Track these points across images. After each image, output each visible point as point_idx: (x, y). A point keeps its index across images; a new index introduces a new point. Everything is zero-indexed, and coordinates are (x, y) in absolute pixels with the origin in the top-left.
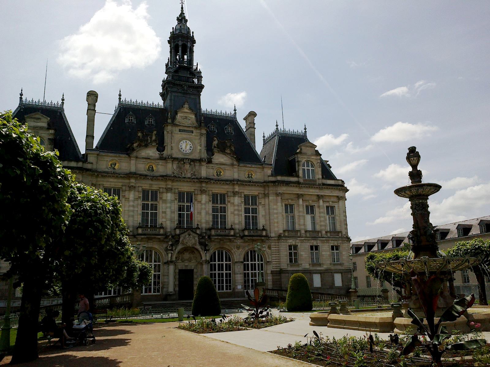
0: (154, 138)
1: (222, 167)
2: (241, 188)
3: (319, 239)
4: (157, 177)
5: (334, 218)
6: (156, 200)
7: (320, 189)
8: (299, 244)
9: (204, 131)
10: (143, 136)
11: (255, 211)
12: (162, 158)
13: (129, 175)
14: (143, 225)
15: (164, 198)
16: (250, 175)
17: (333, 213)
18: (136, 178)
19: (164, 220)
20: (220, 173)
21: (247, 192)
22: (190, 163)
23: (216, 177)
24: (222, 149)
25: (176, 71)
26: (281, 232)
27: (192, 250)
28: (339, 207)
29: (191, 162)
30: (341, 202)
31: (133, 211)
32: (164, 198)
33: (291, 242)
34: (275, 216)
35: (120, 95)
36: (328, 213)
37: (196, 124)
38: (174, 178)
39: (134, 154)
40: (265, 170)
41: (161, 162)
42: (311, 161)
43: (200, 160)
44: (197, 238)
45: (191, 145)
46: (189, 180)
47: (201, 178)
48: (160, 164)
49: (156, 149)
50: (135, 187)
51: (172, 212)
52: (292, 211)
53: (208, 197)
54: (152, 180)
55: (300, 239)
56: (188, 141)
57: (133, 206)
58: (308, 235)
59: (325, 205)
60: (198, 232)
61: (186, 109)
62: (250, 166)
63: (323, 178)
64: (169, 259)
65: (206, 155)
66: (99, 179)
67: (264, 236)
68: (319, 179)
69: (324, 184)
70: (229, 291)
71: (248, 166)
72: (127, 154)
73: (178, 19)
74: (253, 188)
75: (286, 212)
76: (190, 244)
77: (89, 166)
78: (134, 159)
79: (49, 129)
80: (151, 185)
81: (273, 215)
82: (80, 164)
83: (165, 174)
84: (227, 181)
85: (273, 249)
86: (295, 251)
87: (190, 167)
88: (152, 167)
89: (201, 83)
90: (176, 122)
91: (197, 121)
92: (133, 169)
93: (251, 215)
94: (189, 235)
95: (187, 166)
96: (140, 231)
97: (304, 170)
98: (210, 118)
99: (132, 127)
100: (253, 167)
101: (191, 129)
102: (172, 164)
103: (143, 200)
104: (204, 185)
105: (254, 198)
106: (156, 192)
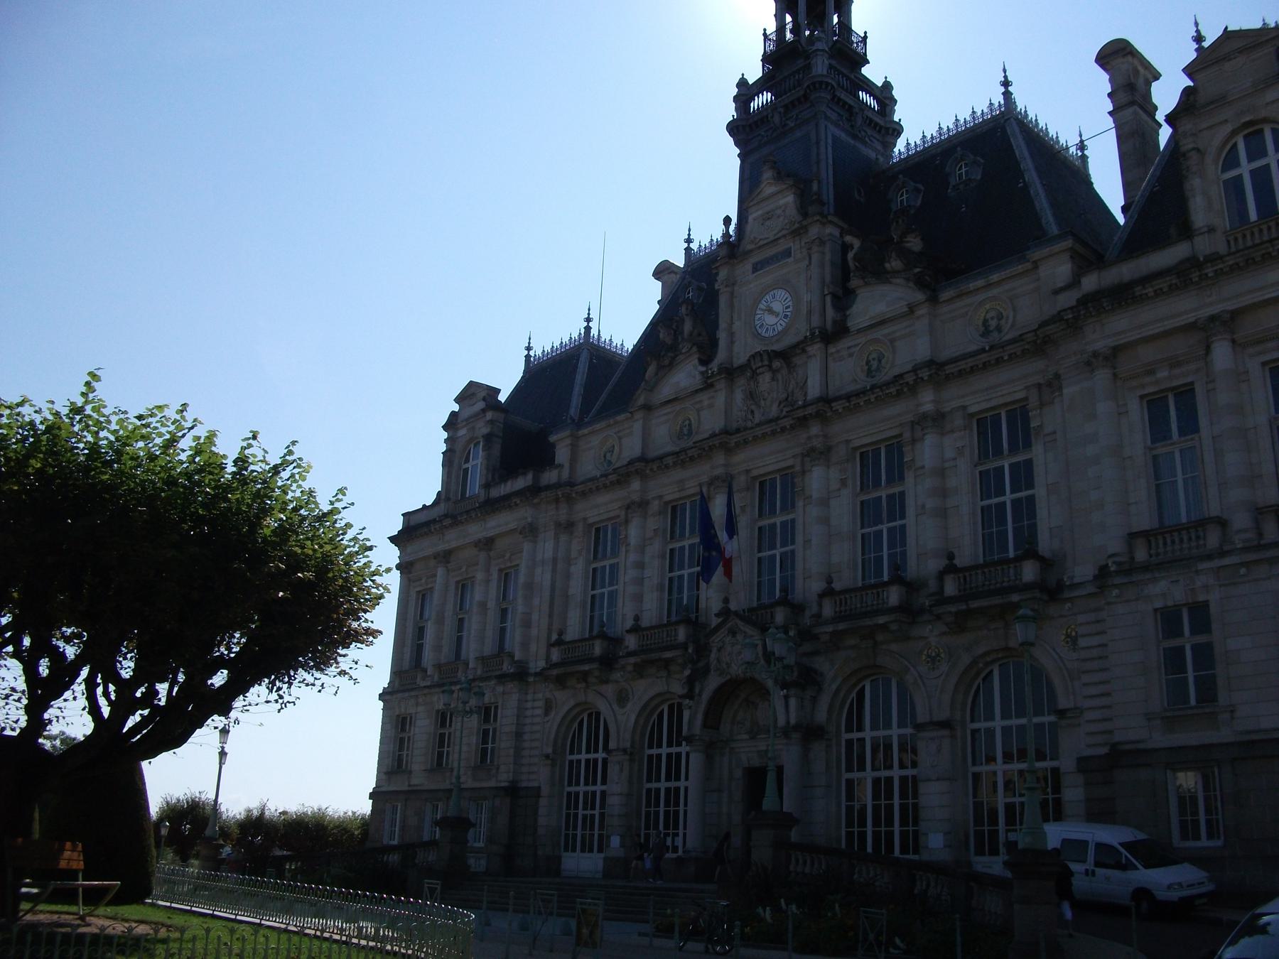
11: (1024, 475)
16: (993, 323)
20: (880, 361)
22: (770, 366)
26: (1116, 545)
29: (770, 361)
40: (1044, 271)
42: (1265, 120)
48: (706, 403)
52: (1190, 424)
62: (980, 283)
67: (1028, 587)
70: (911, 857)
71: (972, 286)
76: (736, 670)
78: (639, 415)
85: (1082, 642)
87: (773, 379)
88: (690, 425)
94: (733, 633)
95: (765, 380)
100: (999, 283)
104: (815, 429)
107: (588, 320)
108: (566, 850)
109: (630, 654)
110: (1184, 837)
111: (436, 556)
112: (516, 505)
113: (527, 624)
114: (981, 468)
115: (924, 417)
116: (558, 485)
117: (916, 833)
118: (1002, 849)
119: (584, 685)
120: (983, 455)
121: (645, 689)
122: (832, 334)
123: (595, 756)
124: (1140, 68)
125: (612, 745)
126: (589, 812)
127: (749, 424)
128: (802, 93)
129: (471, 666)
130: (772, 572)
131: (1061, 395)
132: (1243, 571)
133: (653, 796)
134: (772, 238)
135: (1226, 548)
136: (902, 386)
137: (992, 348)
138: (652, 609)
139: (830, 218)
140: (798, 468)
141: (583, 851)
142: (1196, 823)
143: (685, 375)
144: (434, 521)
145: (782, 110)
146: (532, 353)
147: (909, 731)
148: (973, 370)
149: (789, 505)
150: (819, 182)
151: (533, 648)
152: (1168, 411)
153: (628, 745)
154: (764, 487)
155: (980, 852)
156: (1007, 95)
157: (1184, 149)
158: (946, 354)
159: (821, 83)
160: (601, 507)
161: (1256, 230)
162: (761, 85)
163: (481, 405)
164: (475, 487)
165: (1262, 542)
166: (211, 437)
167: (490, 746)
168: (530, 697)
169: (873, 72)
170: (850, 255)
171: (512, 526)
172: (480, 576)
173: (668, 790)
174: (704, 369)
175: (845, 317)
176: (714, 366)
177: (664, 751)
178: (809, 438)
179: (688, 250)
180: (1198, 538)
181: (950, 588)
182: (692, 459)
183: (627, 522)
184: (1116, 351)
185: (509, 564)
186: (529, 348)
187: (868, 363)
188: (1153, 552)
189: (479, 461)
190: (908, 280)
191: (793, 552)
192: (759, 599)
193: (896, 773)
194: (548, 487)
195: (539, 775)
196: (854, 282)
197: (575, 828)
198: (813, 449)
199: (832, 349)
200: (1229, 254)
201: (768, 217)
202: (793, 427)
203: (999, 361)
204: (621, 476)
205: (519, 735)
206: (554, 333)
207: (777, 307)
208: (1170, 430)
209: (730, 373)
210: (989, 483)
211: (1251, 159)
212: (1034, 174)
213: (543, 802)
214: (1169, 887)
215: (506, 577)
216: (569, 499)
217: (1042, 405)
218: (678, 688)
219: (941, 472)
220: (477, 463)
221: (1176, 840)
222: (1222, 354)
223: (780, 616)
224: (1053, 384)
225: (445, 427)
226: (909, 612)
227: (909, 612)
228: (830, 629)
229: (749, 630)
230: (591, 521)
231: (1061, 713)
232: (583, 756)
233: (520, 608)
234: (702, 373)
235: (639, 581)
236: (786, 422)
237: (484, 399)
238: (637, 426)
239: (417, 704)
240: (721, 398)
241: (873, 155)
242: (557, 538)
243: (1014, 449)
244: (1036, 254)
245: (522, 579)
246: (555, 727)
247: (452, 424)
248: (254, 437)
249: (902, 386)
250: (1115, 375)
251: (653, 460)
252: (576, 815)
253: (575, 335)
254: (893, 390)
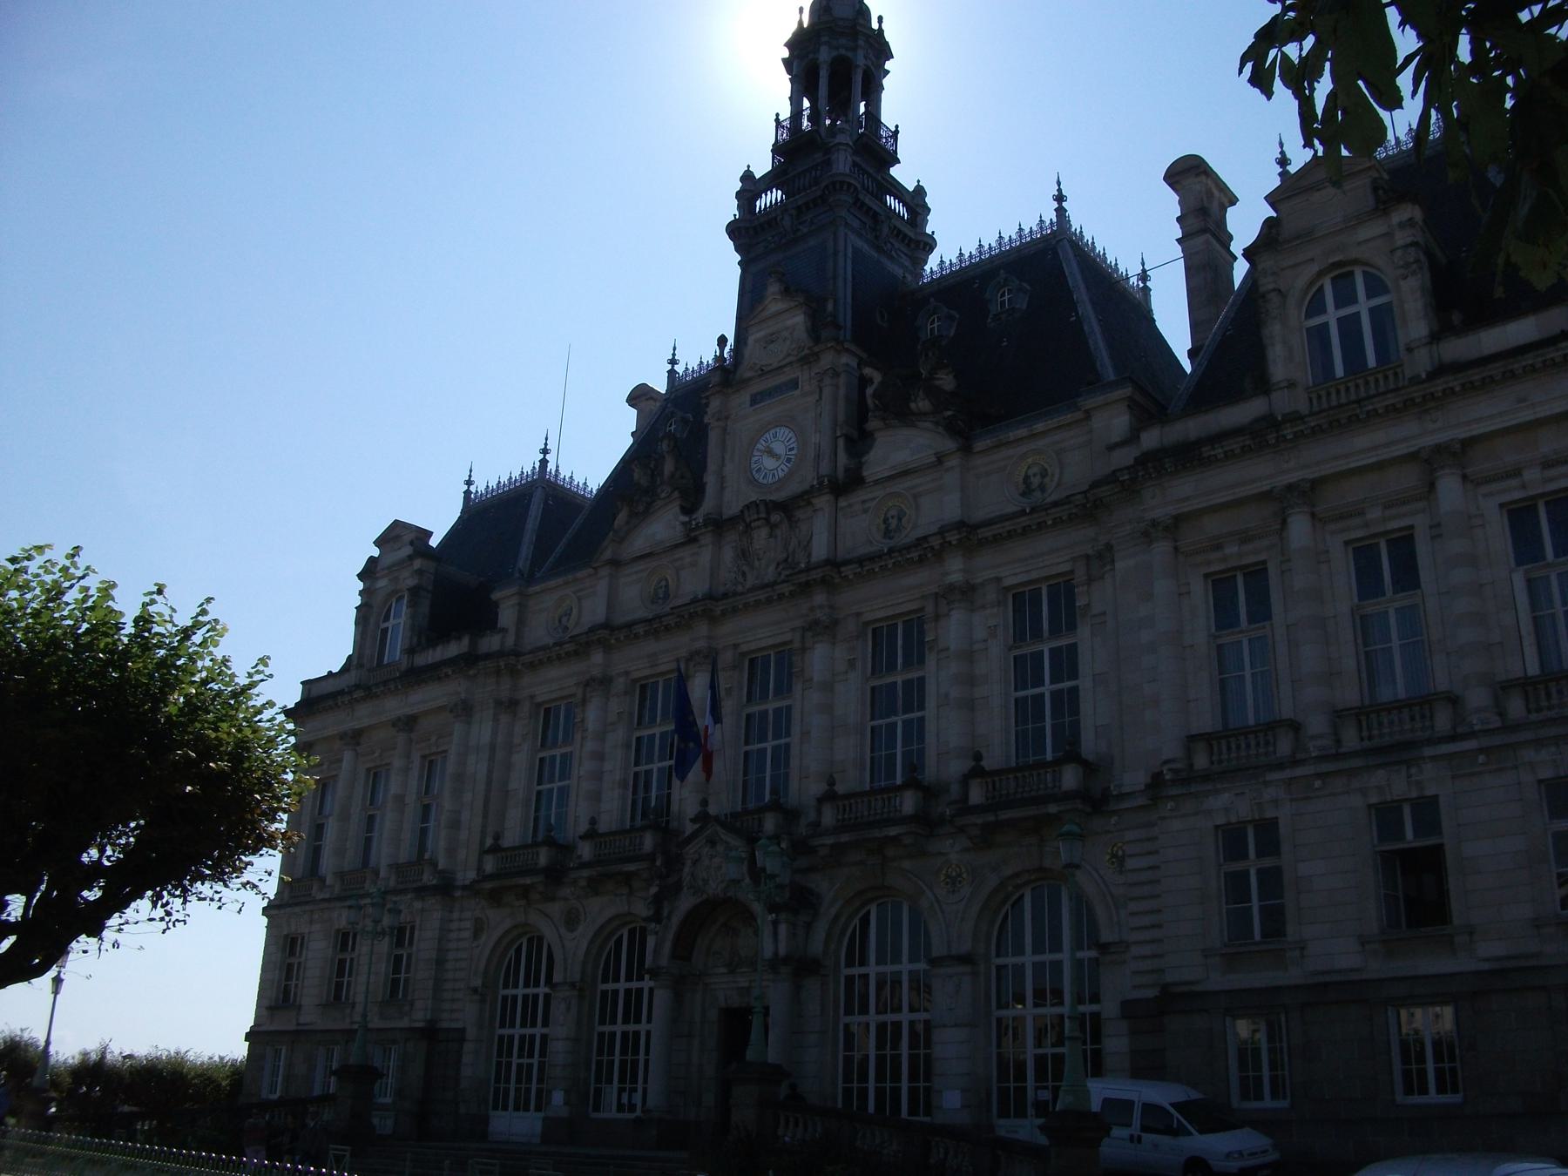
3: (1428, 751)
11: (1066, 663)
20: (900, 519)
22: (767, 520)
29: (768, 513)
42: (1356, 262)
46: (762, 596)
49: (677, 509)
52: (1261, 610)
55: (1288, 773)
62: (1022, 432)
67: (1068, 796)
70: (922, 1118)
71: (1012, 435)
78: (605, 572)
85: (1131, 863)
86: (1268, 862)
87: (771, 536)
88: (667, 586)
94: (712, 842)
95: (761, 536)
100: (1044, 433)
104: (820, 598)
107: (545, 451)
108: (495, 1108)
109: (584, 866)
110: (1245, 1096)
111: (342, 736)
112: (447, 676)
113: (455, 824)
114: (1017, 652)
115: (951, 588)
116: (500, 654)
117: (928, 1090)
118: (1030, 1111)
119: (523, 902)
120: (1019, 637)
121: (600, 909)
122: (846, 484)
123: (535, 990)
124: (1216, 192)
125: (557, 978)
126: (525, 1061)
127: (740, 589)
128: (819, 193)
129: (382, 874)
130: (761, 769)
131: (1113, 569)
132: (1318, 784)
133: (606, 1041)
134: (775, 365)
135: (1299, 756)
136: (926, 551)
137: (1033, 510)
138: (612, 810)
139: (846, 345)
140: (797, 645)
141: (517, 1109)
142: (1259, 1080)
143: (664, 525)
144: (341, 693)
145: (794, 212)
146: (473, 489)
147: (922, 966)
148: (1010, 535)
149: (783, 689)
150: (836, 302)
152: (1236, 593)
153: (577, 977)
154: (755, 664)
155: (1004, 1113)
156: (1061, 211)
157: (1262, 289)
158: (979, 515)
159: (842, 183)
160: (551, 683)
161: (1342, 388)
162: (770, 181)
163: (408, 550)
164: (395, 651)
165: (1342, 750)
166: (107, 589)
167: (403, 976)
168: (456, 915)
169: (903, 174)
170: (869, 391)
172: (397, 763)
173: (625, 1035)
174: (686, 519)
175: (860, 466)
176: (699, 516)
177: (622, 986)
178: (812, 609)
179: (672, 373)
180: (1267, 743)
181: (976, 795)
182: (667, 628)
183: (584, 702)
184: (1178, 519)
185: (434, 749)
186: (469, 483)
187: (886, 521)
188: (1215, 758)
189: (402, 621)
190: (937, 423)
191: (787, 746)
192: (744, 802)
193: (905, 1017)
194: (488, 656)
195: (464, 1014)
196: (873, 424)
197: (508, 1081)
198: (816, 622)
199: (843, 503)
200: (1312, 414)
201: (770, 340)
202: (792, 594)
203: (1041, 526)
204: (582, 645)
205: (440, 963)
206: (502, 466)
207: (779, 448)
208: (1237, 615)
209: (719, 525)
210: (1026, 671)
211: (1338, 305)
212: (1089, 308)
213: (468, 1047)
214: (1228, 1155)
215: (430, 765)
217: (1090, 581)
218: (641, 909)
219: (969, 656)
220: (400, 622)
221: (1236, 1102)
222: (1299, 528)
223: (770, 823)
224: (1104, 557)
225: (361, 576)
226: (926, 822)
227: (926, 822)
228: (829, 841)
230: (539, 700)
231: (1104, 948)
232: (521, 991)
234: (684, 523)
235: (598, 776)
236: (786, 589)
237: (412, 543)
238: (602, 586)
239: (311, 922)
240: (706, 557)
241: (899, 272)
242: (496, 720)
243: (1055, 632)
244: (1088, 403)
246: (487, 952)
247: (369, 572)
248: (160, 592)
249: (926, 551)
250: (1176, 549)
251: (620, 628)
252: (509, 1064)
253: (528, 469)
254: (915, 555)
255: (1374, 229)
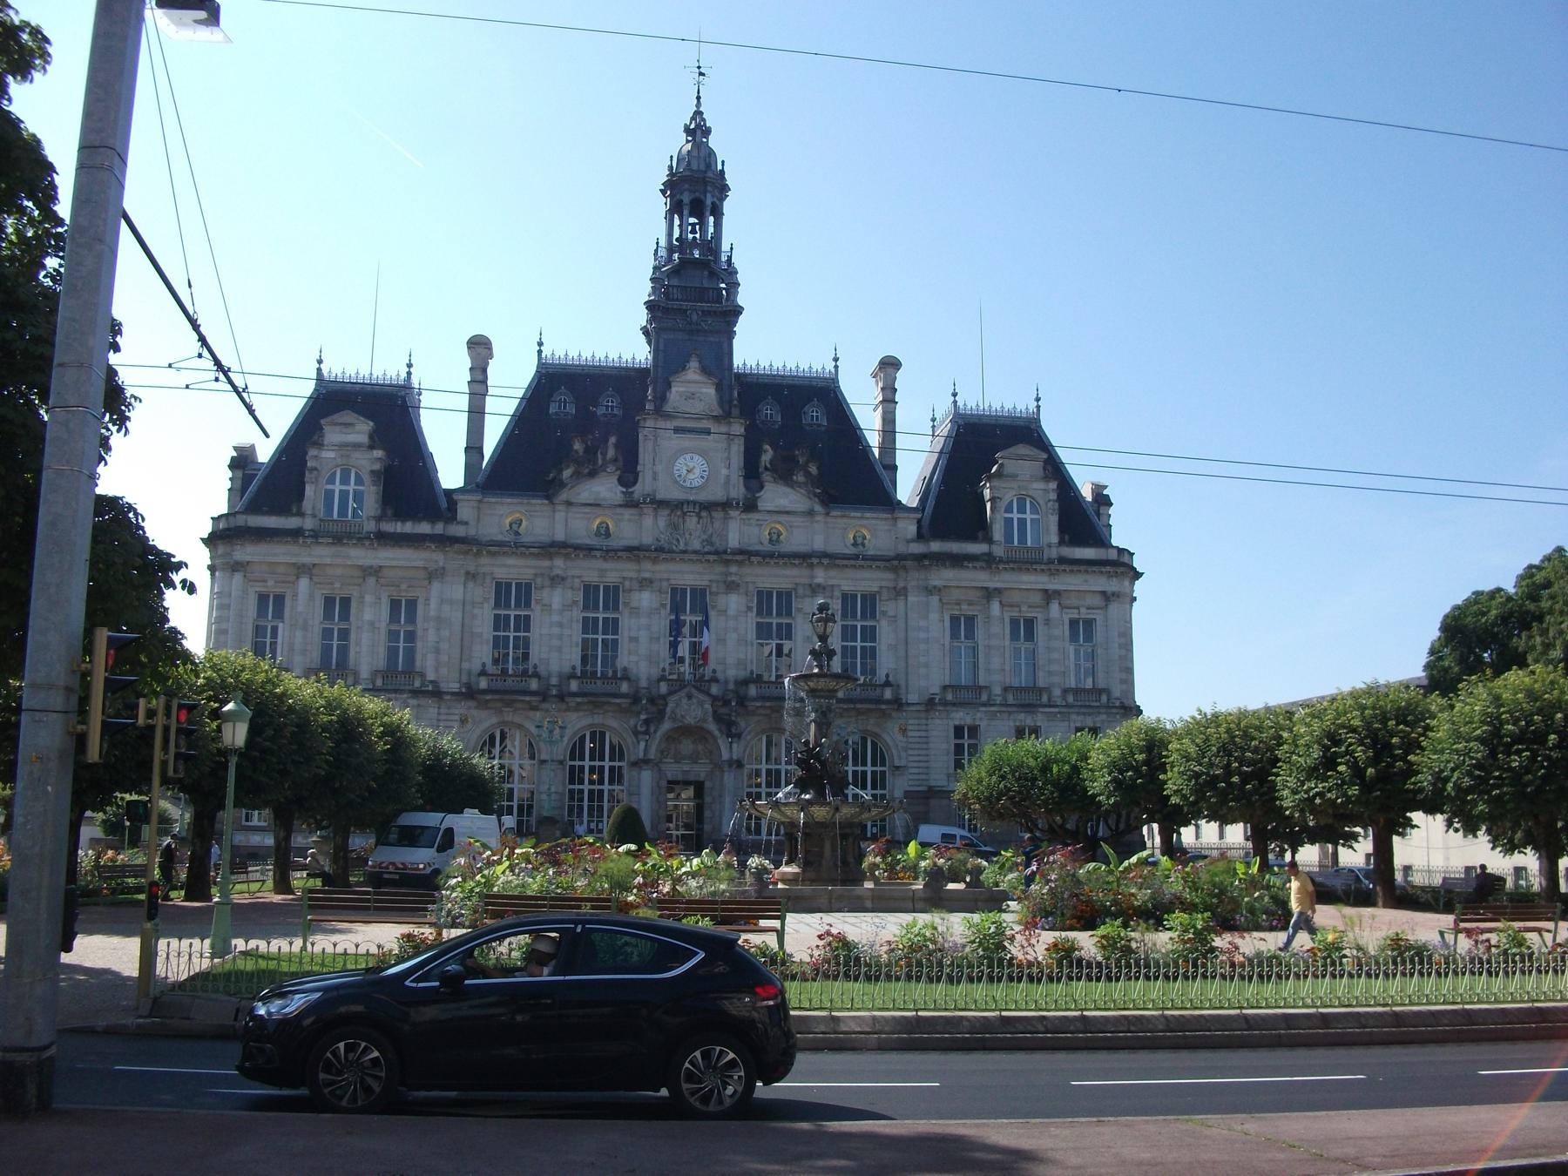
0: (611, 452)
1: (782, 518)
2: (833, 573)
4: (616, 551)
5: (1092, 656)
6: (616, 608)
7: (1052, 573)
8: (983, 724)
9: (738, 428)
10: (587, 450)
11: (870, 634)
12: (630, 503)
13: (551, 549)
14: (587, 675)
15: (634, 604)
17: (1089, 636)
18: (567, 557)
19: (633, 658)
21: (847, 586)
23: (768, 547)
24: (784, 472)
25: (676, 272)
27: (696, 733)
28: (1106, 619)
30: (1114, 608)
31: (560, 637)
32: (634, 604)
33: (961, 717)
34: (922, 646)
35: (540, 344)
36: (1074, 637)
37: (717, 411)
38: (659, 552)
39: (564, 495)
40: (901, 524)
41: (628, 513)
43: (726, 505)
44: (708, 706)
45: (705, 467)
47: (725, 552)
50: (563, 579)
51: (654, 639)
52: (970, 634)
53: (743, 600)
54: (605, 559)
56: (696, 457)
57: (561, 625)
58: (1011, 700)
59: (1066, 618)
60: (714, 690)
61: (692, 373)
63: (1061, 542)
64: (641, 755)
65: (742, 490)
66: (484, 560)
67: (888, 702)
68: (1049, 546)
69: (1063, 560)
72: (548, 498)
73: (687, 130)
74: (866, 574)
75: (955, 635)
76: (690, 720)
77: (456, 530)
79: (371, 447)
80: (602, 572)
81: (916, 643)
82: (439, 528)
83: (635, 543)
84: (795, 555)
89: (735, 300)
90: (668, 408)
91: (721, 402)
92: (560, 536)
93: (859, 644)
94: (690, 697)
95: (692, 522)
96: (574, 686)
97: (1009, 522)
98: (766, 385)
99: (571, 421)
101: (705, 424)
102: (656, 516)
103: (586, 608)
104: (734, 569)
105: (870, 601)
106: (616, 588)
113: (437, 651)
151: (444, 671)
171: (420, 564)
199: (744, 516)
216: (478, 554)
222: (995, 607)
229: (701, 697)
233: (432, 636)
245: (432, 613)
255: (1041, 485)
